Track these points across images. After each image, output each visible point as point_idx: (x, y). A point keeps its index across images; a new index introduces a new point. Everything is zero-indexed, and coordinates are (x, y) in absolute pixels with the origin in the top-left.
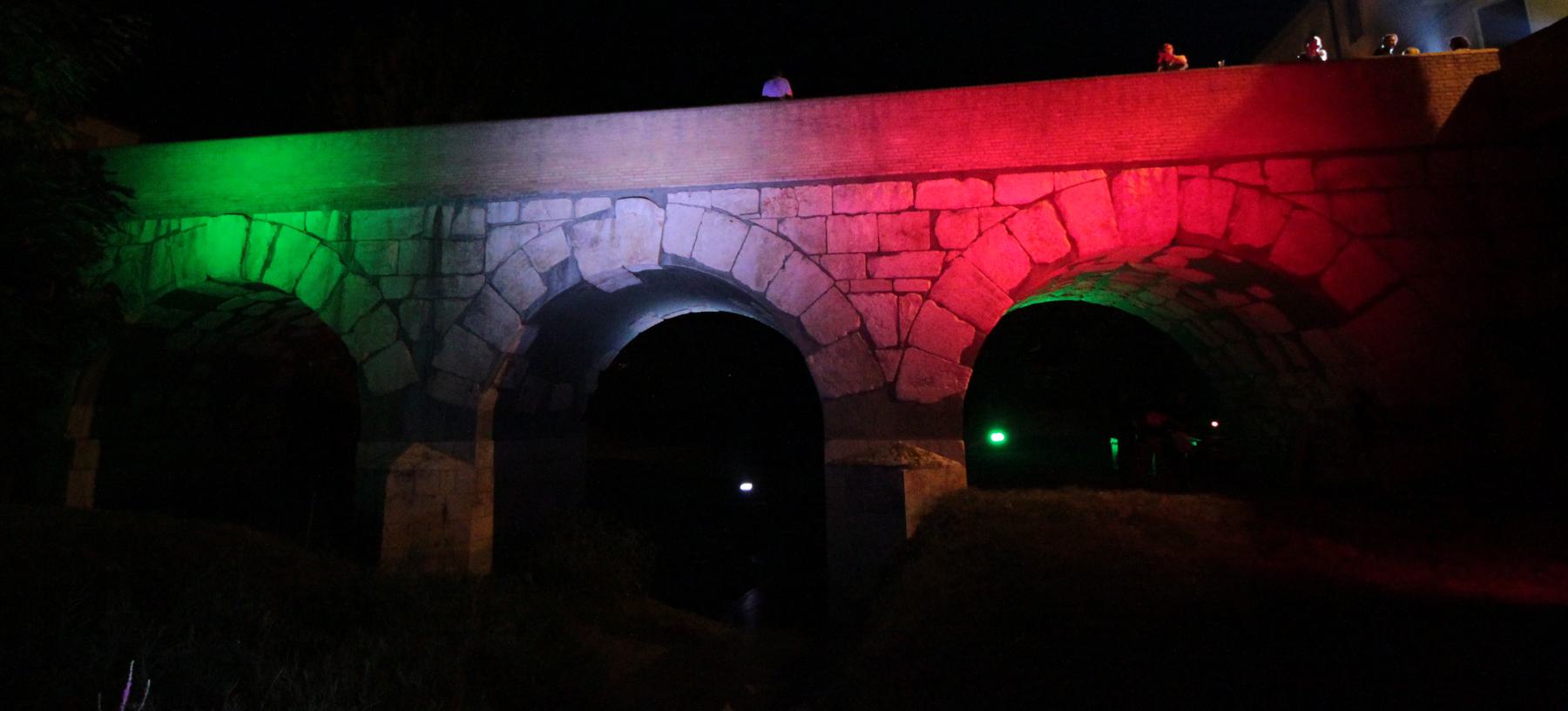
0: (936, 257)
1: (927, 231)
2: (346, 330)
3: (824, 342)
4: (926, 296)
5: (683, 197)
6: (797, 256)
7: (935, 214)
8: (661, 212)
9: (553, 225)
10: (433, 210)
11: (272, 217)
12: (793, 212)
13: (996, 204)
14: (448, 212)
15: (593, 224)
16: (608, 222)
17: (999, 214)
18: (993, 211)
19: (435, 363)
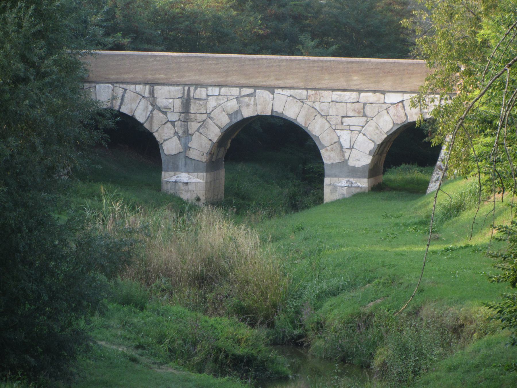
0: (364, 119)
1: (362, 111)
2: (155, 131)
3: (326, 145)
4: (360, 132)
5: (280, 91)
6: (319, 116)
7: (365, 104)
8: (271, 96)
9: (232, 98)
10: (186, 88)
11: (124, 86)
12: (318, 100)
13: (384, 103)
14: (192, 89)
15: (247, 99)
16: (253, 98)
17: (385, 106)
18: (383, 105)
19: (190, 145)
